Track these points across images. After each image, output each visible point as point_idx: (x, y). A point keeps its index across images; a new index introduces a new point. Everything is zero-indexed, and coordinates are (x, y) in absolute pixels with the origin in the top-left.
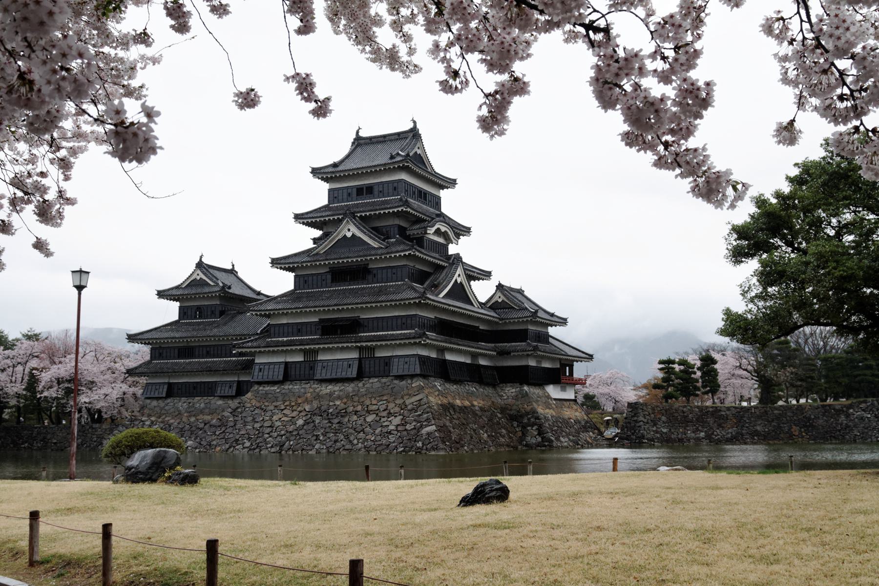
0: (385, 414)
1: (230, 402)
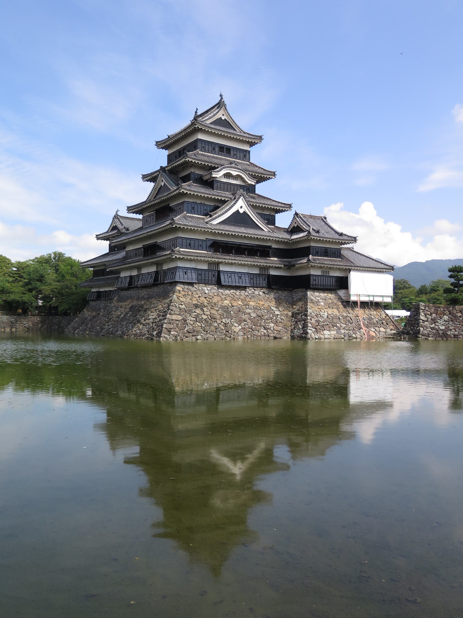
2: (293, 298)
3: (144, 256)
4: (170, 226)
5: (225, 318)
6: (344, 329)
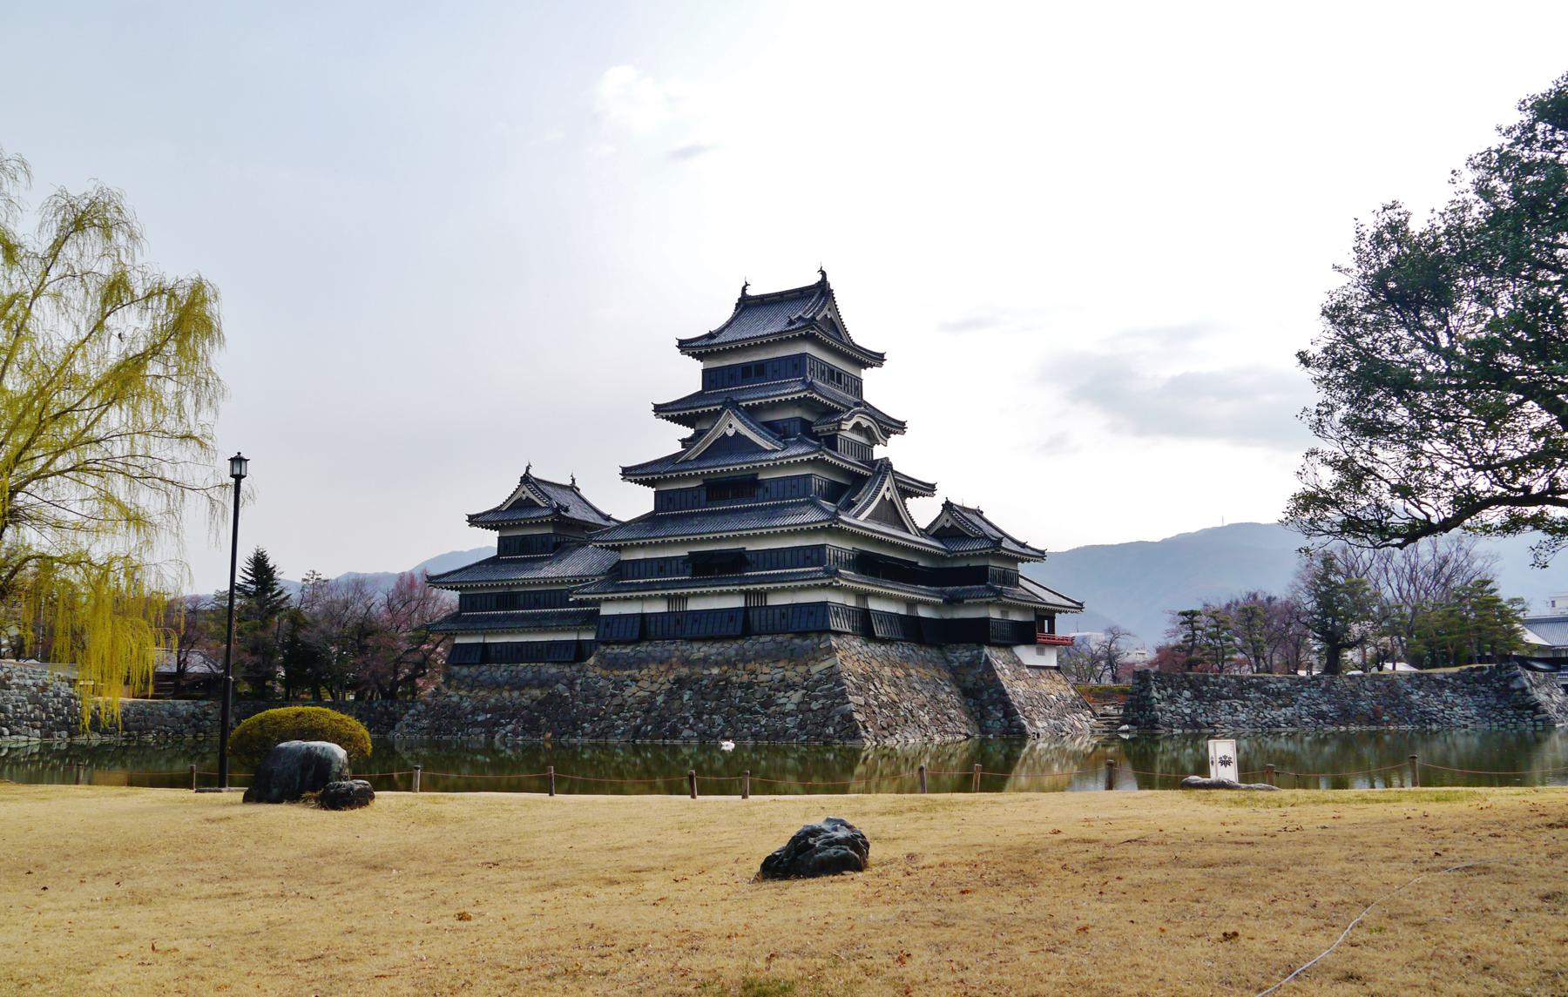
1: (567, 670)
2: (949, 662)
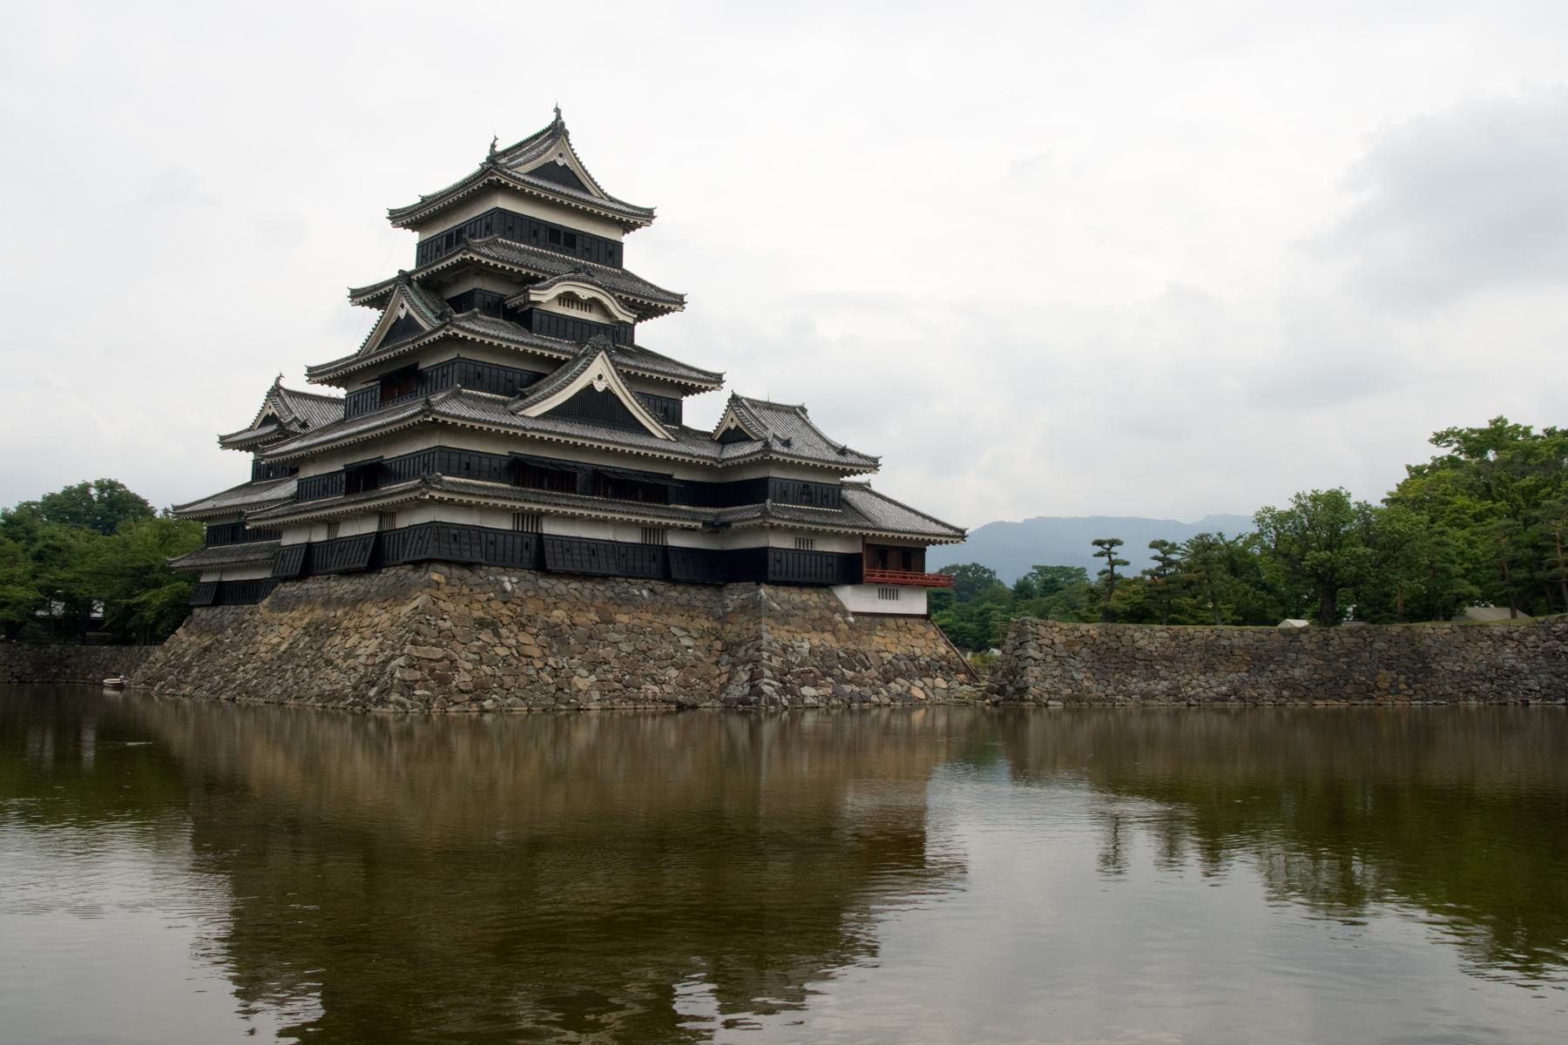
0: (368, 633)
3: (347, 493)
4: (420, 418)
5: (554, 655)
6: (850, 682)
